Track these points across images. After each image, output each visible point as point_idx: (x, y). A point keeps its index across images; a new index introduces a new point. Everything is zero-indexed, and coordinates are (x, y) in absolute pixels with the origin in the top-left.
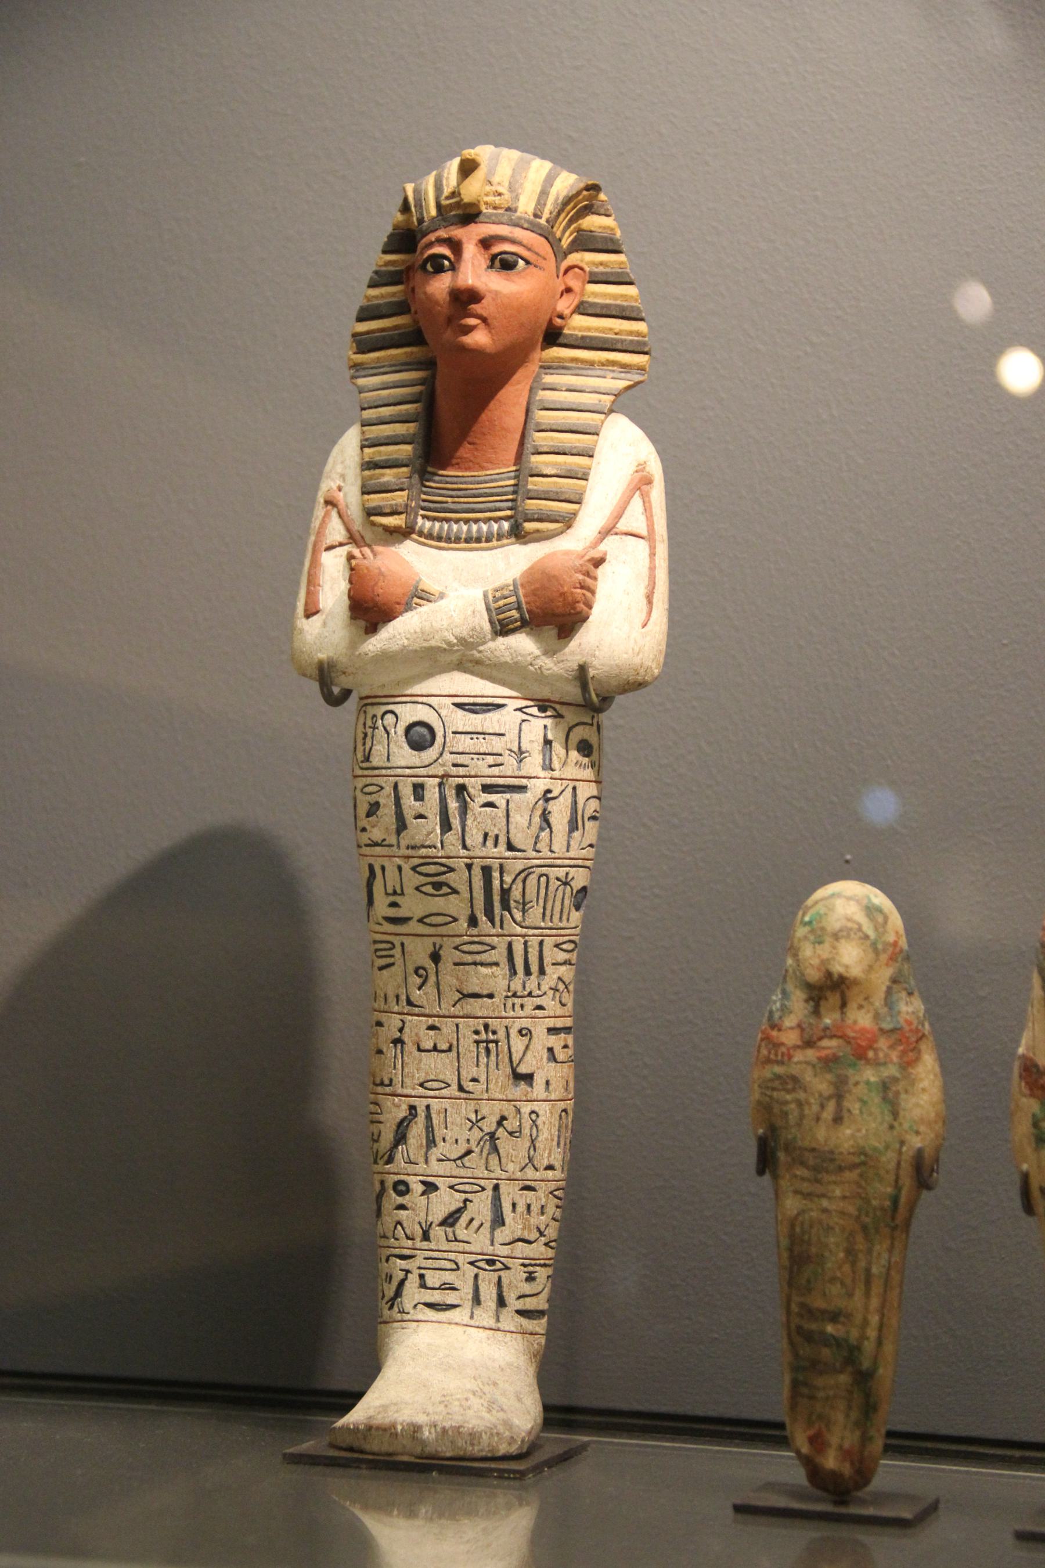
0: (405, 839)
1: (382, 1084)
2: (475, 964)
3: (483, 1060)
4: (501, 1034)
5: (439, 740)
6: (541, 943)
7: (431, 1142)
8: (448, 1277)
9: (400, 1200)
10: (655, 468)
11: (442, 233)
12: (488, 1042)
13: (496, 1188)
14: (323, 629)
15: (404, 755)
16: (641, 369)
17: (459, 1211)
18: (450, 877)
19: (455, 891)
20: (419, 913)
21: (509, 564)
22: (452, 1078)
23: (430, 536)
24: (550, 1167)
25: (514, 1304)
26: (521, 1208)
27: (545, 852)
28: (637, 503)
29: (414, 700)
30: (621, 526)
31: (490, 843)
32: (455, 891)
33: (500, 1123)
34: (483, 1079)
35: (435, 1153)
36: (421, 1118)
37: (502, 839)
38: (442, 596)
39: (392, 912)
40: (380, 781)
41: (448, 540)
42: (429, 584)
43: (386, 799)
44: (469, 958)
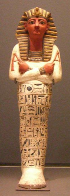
0: (27, 103)
1: (22, 136)
2: (36, 120)
3: (37, 133)
4: (40, 129)
5: (32, 89)
6: (45, 117)
7: (29, 144)
8: (32, 162)
9: (25, 151)
10: (59, 51)
11: (33, 18)
12: (38, 130)
13: (39, 150)
14: (15, 73)
15: (27, 91)
16: (57, 38)
17: (34, 153)
18: (33, 108)
19: (34, 110)
20: (29, 113)
21: (42, 65)
22: (33, 136)
23: (30, 60)
24: (46, 146)
25: (42, 165)
26: (42, 152)
27: (46, 105)
28: (57, 57)
29: (29, 83)
30: (56, 59)
31: (39, 104)
32: (34, 110)
33: (39, 141)
34: (37, 135)
35: (30, 145)
36: (28, 141)
37: (41, 103)
38: (32, 69)
39: (24, 113)
40: (23, 95)
41: (33, 61)
42: (31, 67)
43: (24, 97)
44: (35, 119)
